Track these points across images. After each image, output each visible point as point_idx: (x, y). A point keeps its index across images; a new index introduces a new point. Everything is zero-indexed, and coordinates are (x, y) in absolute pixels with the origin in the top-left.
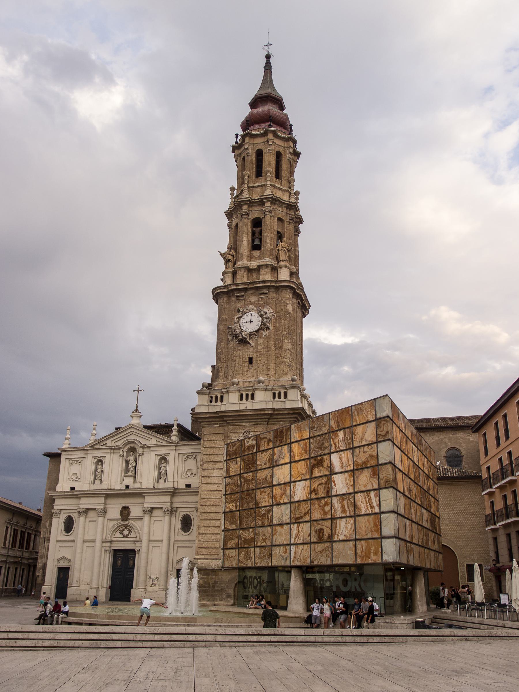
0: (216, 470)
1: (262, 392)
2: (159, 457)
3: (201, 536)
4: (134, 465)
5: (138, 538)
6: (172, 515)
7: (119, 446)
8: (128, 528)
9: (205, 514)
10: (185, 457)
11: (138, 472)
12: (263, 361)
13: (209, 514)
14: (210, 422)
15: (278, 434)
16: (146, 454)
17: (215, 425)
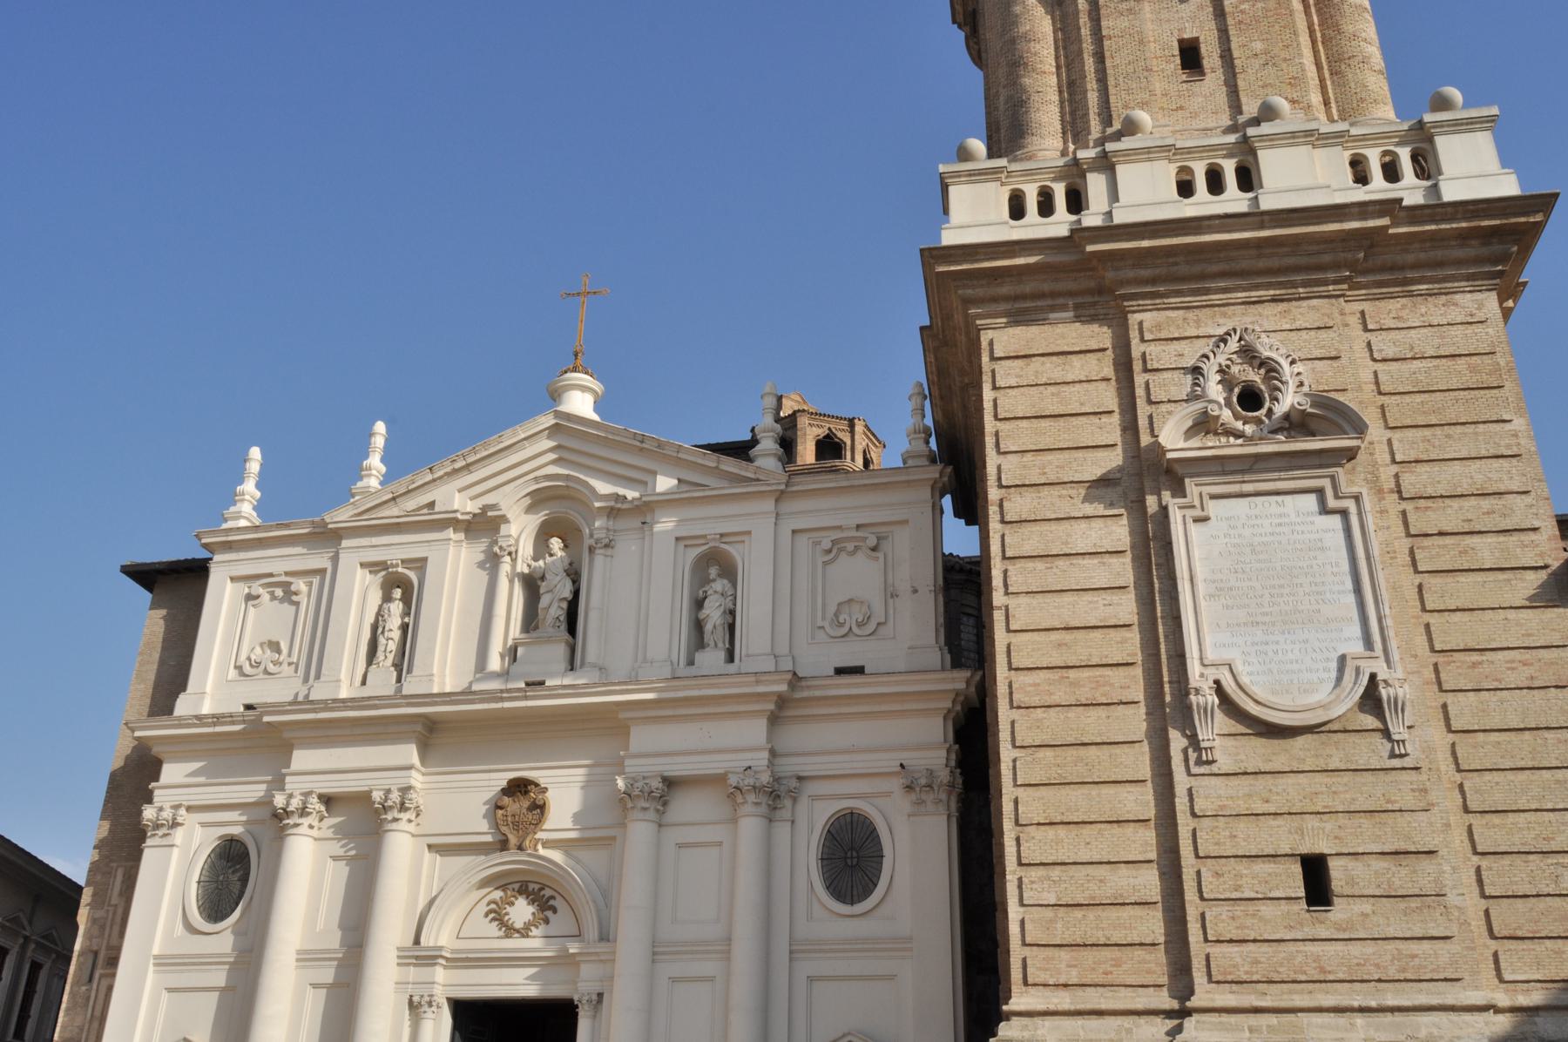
0: (1083, 525)
1: (1301, 154)
2: (694, 553)
3: (1034, 873)
4: (567, 592)
5: (592, 932)
6: (779, 814)
7: (493, 507)
8: (531, 886)
9: (1049, 753)
10: (826, 544)
11: (590, 620)
12: (1258, 46)
13: (1072, 751)
14: (1024, 297)
15: (1148, 536)
16: (628, 547)
17: (1052, 316)
